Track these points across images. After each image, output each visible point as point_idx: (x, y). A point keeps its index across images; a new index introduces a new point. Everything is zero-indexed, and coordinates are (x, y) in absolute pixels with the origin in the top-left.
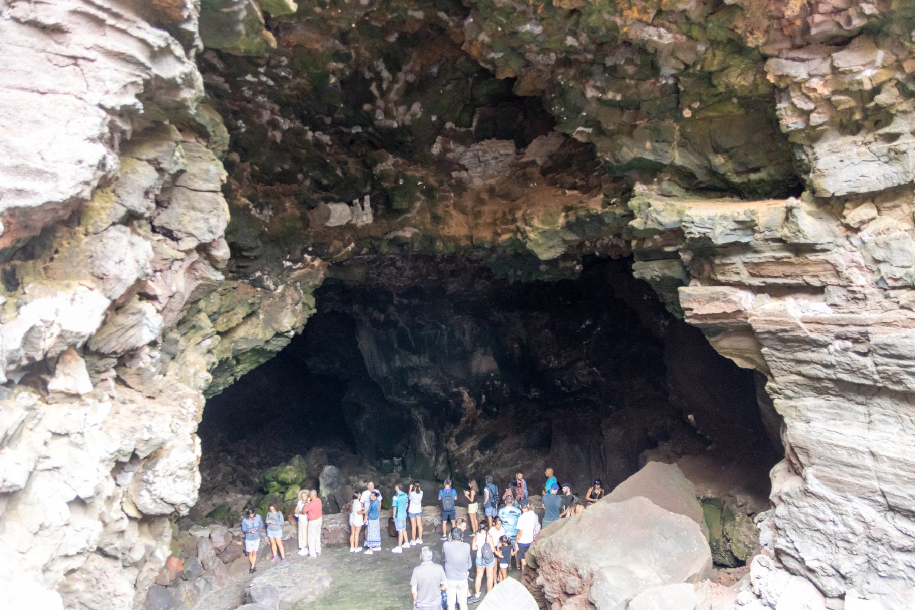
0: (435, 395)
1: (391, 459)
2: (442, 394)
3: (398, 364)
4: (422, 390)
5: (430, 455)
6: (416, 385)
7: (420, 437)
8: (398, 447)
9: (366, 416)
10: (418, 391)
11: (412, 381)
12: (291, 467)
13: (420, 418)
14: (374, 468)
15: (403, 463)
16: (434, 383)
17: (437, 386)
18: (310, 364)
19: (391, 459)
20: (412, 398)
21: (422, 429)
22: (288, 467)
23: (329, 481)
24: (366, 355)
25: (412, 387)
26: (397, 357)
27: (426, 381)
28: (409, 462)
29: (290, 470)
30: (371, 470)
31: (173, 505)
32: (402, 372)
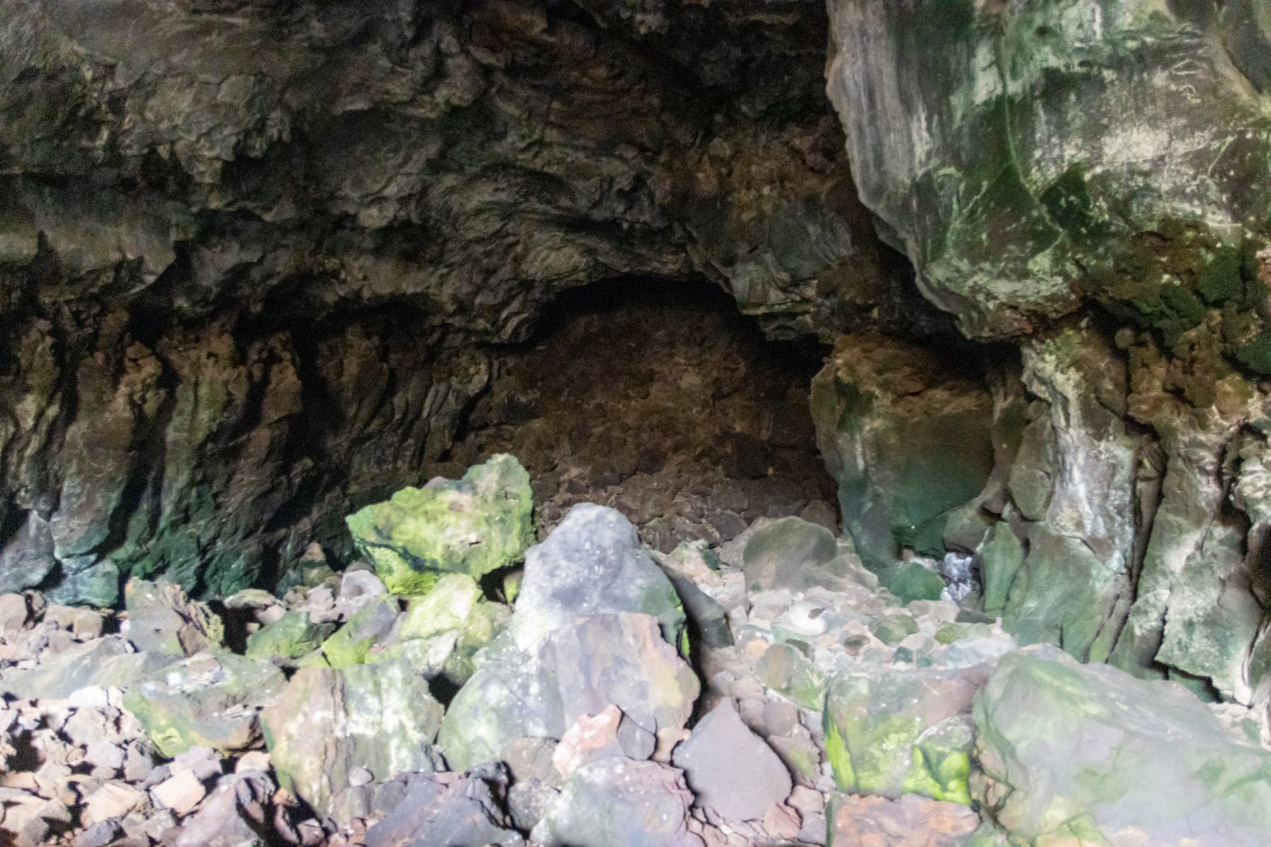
0: (1170, 235)
1: (939, 558)
2: (1219, 222)
3: (985, 86)
4: (1100, 209)
5: (1099, 546)
6: (1072, 180)
7: (1059, 470)
8: (964, 519)
9: (871, 425)
10: (1075, 218)
11: (1050, 156)
12: (465, 498)
13: (1068, 383)
14: (873, 578)
15: (978, 574)
16: (1181, 148)
17: (1198, 159)
18: (740, 286)
19: (939, 558)
20: (1042, 262)
21: (1073, 435)
22: (451, 496)
23: (568, 574)
24: (849, 117)
25: (1050, 195)
26: (983, 55)
27: (1133, 145)
28: (1000, 567)
29: (455, 507)
30: (860, 580)
31: (514, 601)
32: (1002, 115)
